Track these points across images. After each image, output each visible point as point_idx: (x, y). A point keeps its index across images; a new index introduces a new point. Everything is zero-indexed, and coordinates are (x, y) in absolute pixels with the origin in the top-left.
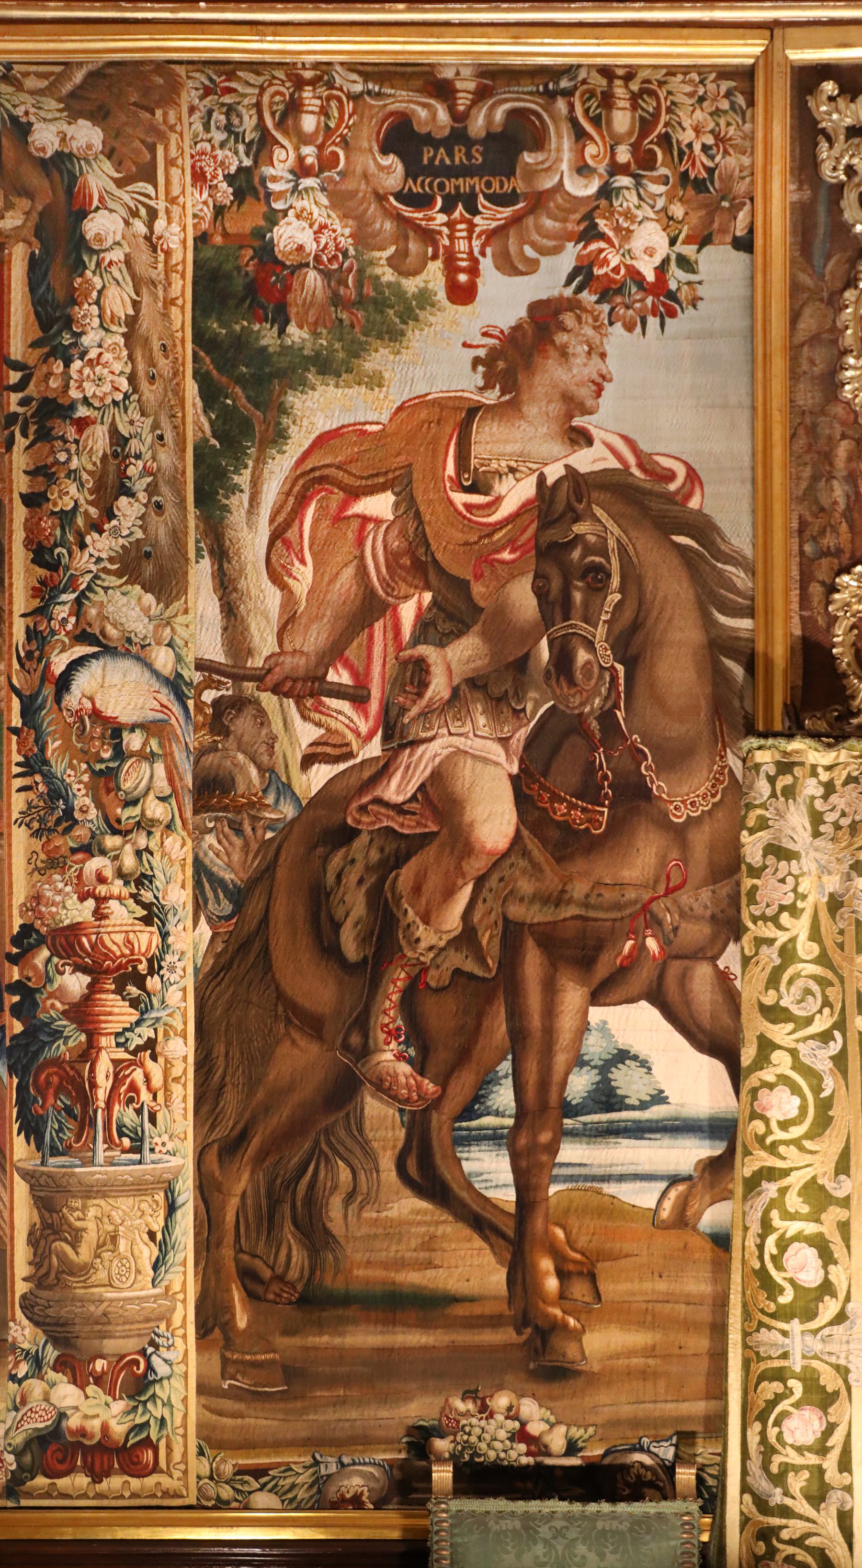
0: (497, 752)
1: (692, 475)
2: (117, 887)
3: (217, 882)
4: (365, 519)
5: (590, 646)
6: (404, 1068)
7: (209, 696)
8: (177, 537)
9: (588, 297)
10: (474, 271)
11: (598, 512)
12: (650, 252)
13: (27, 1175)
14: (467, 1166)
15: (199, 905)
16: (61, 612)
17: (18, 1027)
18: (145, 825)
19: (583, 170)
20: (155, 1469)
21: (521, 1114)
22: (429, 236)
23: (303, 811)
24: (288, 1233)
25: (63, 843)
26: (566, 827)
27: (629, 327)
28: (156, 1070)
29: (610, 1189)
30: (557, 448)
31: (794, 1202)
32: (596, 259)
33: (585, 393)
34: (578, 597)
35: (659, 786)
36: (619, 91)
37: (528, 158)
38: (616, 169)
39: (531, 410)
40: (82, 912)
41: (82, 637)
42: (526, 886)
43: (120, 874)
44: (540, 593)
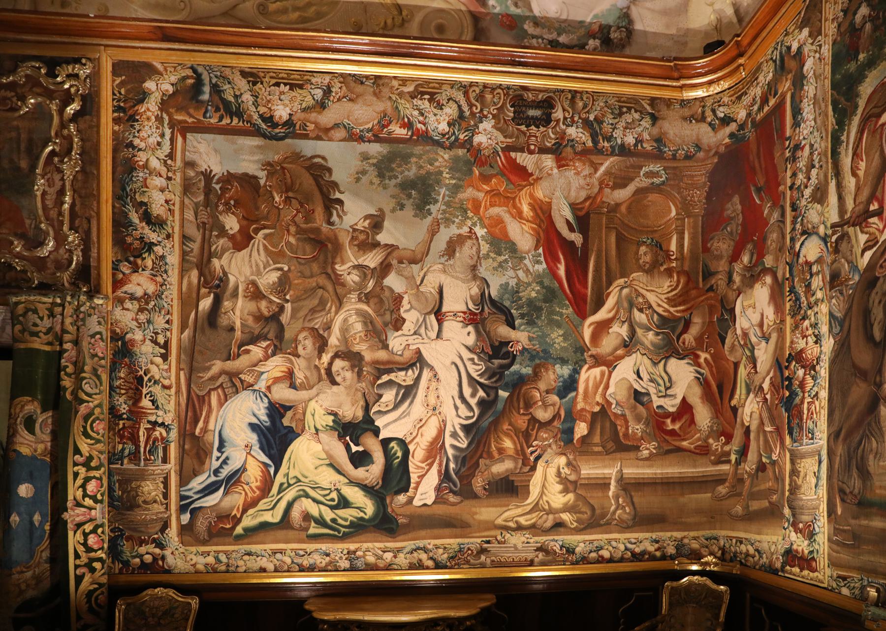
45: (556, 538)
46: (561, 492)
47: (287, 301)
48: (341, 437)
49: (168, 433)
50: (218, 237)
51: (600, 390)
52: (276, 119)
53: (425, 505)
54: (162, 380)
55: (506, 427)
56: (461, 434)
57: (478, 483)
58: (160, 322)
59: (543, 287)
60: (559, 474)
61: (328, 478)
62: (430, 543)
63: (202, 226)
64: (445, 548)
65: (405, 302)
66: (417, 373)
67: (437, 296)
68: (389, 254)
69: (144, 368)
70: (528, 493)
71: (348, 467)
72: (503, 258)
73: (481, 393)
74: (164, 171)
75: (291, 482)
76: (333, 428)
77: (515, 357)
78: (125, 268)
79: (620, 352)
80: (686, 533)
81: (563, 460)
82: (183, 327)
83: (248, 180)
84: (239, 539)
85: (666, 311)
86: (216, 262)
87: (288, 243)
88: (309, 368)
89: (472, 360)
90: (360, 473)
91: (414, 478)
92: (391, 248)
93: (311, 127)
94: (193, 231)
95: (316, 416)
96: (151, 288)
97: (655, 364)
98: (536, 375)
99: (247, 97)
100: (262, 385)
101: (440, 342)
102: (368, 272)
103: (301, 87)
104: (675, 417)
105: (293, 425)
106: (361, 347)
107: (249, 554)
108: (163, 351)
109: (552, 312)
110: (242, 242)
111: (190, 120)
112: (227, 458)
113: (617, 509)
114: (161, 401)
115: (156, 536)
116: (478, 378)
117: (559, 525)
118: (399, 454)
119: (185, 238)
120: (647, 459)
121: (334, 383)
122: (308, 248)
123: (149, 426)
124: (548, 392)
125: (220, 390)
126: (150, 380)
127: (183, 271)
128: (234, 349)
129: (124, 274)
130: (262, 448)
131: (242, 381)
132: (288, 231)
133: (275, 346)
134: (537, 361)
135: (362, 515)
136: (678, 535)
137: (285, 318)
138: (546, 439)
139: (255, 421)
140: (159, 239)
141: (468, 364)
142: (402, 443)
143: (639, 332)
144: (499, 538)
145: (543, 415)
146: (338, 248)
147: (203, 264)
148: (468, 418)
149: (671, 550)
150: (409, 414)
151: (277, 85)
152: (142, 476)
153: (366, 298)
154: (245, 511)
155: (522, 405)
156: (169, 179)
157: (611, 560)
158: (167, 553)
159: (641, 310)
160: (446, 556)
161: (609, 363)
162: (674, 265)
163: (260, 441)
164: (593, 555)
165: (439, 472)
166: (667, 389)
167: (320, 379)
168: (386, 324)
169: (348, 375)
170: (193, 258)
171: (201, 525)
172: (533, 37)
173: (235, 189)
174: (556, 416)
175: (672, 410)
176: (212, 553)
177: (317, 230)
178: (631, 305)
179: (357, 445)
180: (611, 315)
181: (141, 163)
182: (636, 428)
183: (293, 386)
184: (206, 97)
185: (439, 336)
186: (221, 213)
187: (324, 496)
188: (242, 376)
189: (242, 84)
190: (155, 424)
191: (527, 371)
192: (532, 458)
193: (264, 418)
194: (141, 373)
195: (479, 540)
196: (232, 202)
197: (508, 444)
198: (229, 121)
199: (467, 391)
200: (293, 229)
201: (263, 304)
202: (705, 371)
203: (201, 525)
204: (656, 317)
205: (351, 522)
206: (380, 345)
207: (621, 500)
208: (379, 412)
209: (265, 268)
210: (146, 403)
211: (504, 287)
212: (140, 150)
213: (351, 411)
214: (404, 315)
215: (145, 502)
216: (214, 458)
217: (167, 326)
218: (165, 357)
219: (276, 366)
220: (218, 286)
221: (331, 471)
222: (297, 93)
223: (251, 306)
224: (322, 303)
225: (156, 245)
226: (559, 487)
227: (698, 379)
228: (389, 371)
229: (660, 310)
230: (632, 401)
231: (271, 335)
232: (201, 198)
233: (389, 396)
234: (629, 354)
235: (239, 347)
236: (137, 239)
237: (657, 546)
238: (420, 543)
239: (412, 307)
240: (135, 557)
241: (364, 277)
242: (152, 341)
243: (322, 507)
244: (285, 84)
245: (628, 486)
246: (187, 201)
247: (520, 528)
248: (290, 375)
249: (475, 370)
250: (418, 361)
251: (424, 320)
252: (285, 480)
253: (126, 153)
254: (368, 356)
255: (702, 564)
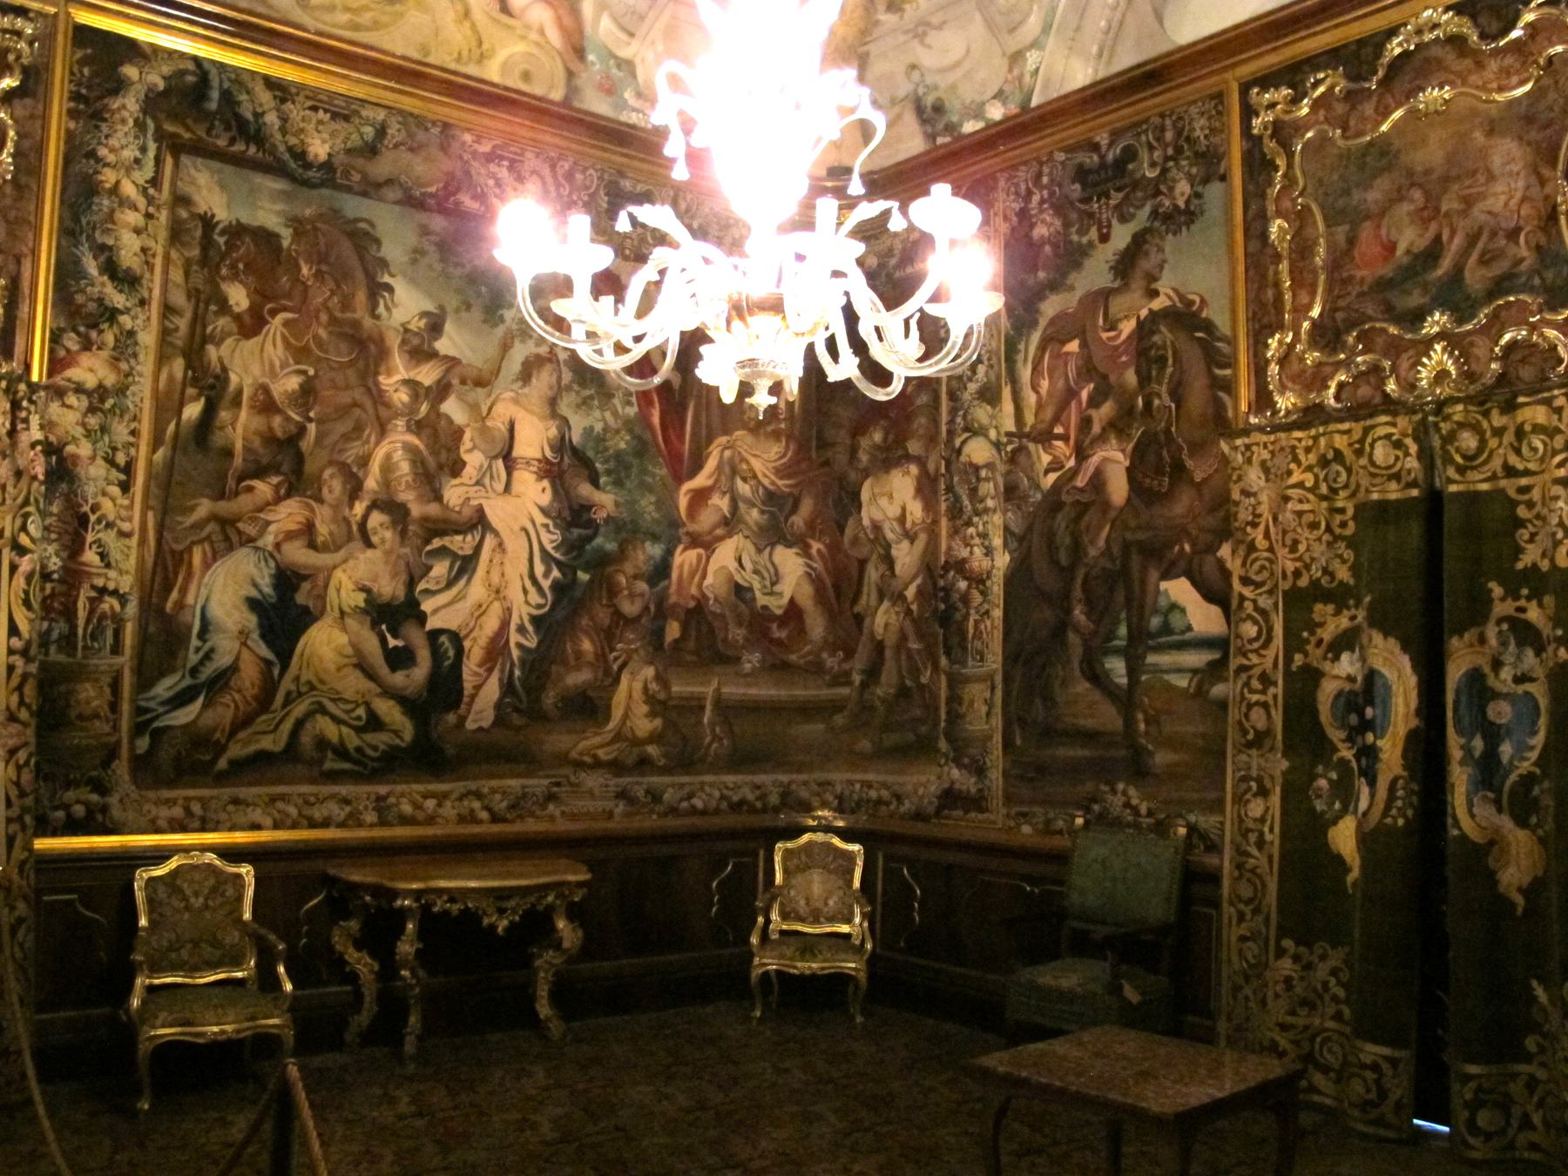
0: (1119, 456)
1: (1203, 301)
2: (977, 541)
3: (1012, 534)
4: (1068, 354)
5: (1159, 396)
6: (1083, 618)
7: (1009, 448)
8: (999, 377)
9: (1157, 224)
10: (1109, 226)
11: (1163, 329)
12: (1182, 194)
13: (946, 673)
14: (1107, 666)
15: (1006, 545)
16: (959, 420)
17: (943, 607)
18: (986, 510)
19: (1153, 165)
20: (987, 810)
21: (1131, 637)
22: (1091, 215)
23: (1044, 496)
24: (1038, 701)
25: (959, 522)
26: (1150, 489)
27: (1175, 234)
28: (988, 623)
29: (1166, 677)
30: (1144, 301)
31: (1256, 684)
32: (1161, 205)
33: (1155, 272)
34: (1154, 373)
35: (1189, 463)
36: (1168, 122)
37: (1130, 167)
38: (1167, 159)
39: (1133, 286)
40: (965, 553)
41: (966, 429)
42: (1133, 523)
43: (979, 535)
44: (1138, 373)
45: (640, 779)
46: (647, 716)
47: (310, 420)
48: (375, 625)
49: (123, 604)
50: (217, 314)
51: (697, 579)
52: (311, 157)
53: (481, 729)
54: (118, 522)
55: (585, 621)
56: (530, 628)
57: (550, 699)
58: (121, 431)
59: (635, 437)
60: (645, 689)
61: (354, 683)
62: (485, 785)
63: (193, 294)
64: (504, 793)
65: (467, 436)
66: (478, 538)
67: (507, 435)
68: (448, 371)
69: (91, 501)
70: (608, 718)
71: (383, 669)
72: (587, 392)
73: (556, 573)
74: (141, 202)
75: (304, 689)
76: (365, 611)
77: (598, 526)
78: (71, 342)
79: (719, 532)
80: (794, 776)
81: (650, 672)
82: (157, 442)
83: (266, 238)
84: (221, 779)
85: (773, 483)
86: (212, 351)
87: (316, 337)
88: (334, 520)
89: (546, 526)
90: (398, 679)
91: (468, 687)
92: (452, 362)
93: (356, 177)
94: (179, 298)
95: (343, 593)
96: (110, 379)
97: (759, 551)
98: (621, 555)
99: (271, 119)
100: (268, 540)
101: (508, 498)
102: (422, 392)
103: (346, 118)
104: (783, 620)
105: (311, 605)
106: (407, 496)
107: (236, 801)
108: (123, 477)
109: (644, 472)
110: (251, 325)
111: (187, 135)
112: (212, 650)
113: (713, 741)
114: (115, 556)
115: (94, 773)
116: (552, 552)
117: (644, 764)
118: (451, 653)
119: (168, 310)
120: (746, 675)
121: (369, 544)
122: (344, 347)
123: (93, 594)
124: (635, 577)
125: (207, 547)
126: (99, 521)
127: (162, 359)
128: (231, 483)
129: (68, 351)
130: (263, 636)
131: (239, 532)
132: (317, 318)
133: (291, 484)
134: (624, 535)
135: (398, 741)
136: (784, 778)
137: (306, 444)
138: (631, 642)
139: (254, 593)
140: (128, 304)
141: (542, 532)
142: (456, 638)
143: (742, 505)
144: (573, 778)
145: (630, 608)
146: (383, 353)
147: (194, 353)
148: (539, 606)
149: (774, 799)
150: (464, 597)
151: (314, 109)
152: (77, 674)
153: (417, 427)
154: (233, 733)
155: (604, 593)
156: (149, 216)
157: (704, 813)
158: (113, 800)
159: (744, 480)
160: (504, 804)
161: (707, 544)
162: (783, 426)
163: (261, 625)
164: (685, 804)
165: (501, 680)
166: (773, 584)
167: (350, 538)
168: (441, 467)
169: (388, 534)
170: (179, 340)
171: (166, 754)
172: (634, 110)
173: (246, 247)
174: (646, 608)
175: (779, 612)
176: (180, 802)
177: (356, 324)
178: (734, 472)
179: (395, 636)
180: (710, 482)
181: (107, 186)
182: (737, 634)
183: (312, 545)
184: (213, 105)
185: (507, 488)
186: (223, 279)
187: (348, 712)
188: (240, 525)
189: (265, 97)
190: (103, 591)
191: (611, 546)
192: (615, 667)
193: (268, 590)
194: (86, 508)
195: (546, 782)
196: (241, 266)
197: (587, 646)
198: (243, 148)
199: (539, 569)
200: (324, 317)
201: (277, 421)
202: (818, 565)
203: (166, 754)
204: (761, 491)
205: (384, 752)
206: (432, 495)
207: (718, 730)
208: (427, 592)
209: (282, 367)
210: (90, 556)
211: (588, 431)
212: (107, 165)
213: (390, 588)
214: (465, 457)
215: (81, 717)
216: (192, 649)
217: (132, 439)
218: (125, 487)
219: (288, 514)
220: (212, 387)
221: (358, 673)
222: (339, 126)
223: (258, 422)
224: (358, 429)
225: (122, 313)
226: (645, 709)
227: (809, 575)
228: (442, 533)
229: (766, 482)
230: (733, 598)
231: (285, 468)
232: (195, 252)
233: (440, 569)
234: (730, 535)
235: (240, 479)
236: (91, 299)
237: (758, 793)
238: (472, 785)
239: (474, 447)
240: (56, 808)
241: (415, 396)
242: (106, 459)
243: (345, 730)
244: (326, 111)
245: (726, 709)
246: (174, 254)
247: (598, 764)
248: (309, 529)
249: (551, 539)
250: (479, 522)
251: (490, 467)
252: (293, 688)
253: (87, 166)
254: (416, 510)
255: (814, 818)
